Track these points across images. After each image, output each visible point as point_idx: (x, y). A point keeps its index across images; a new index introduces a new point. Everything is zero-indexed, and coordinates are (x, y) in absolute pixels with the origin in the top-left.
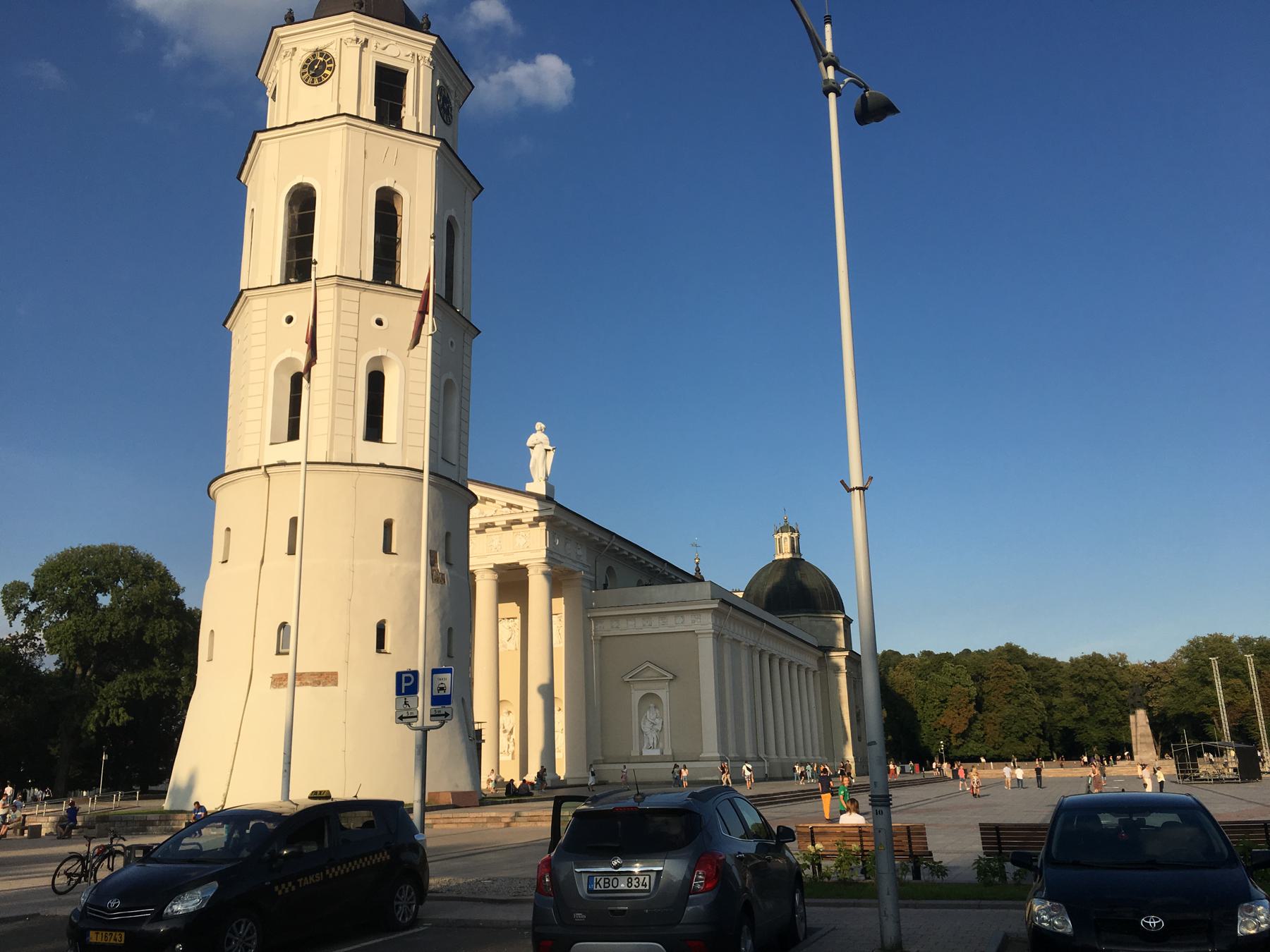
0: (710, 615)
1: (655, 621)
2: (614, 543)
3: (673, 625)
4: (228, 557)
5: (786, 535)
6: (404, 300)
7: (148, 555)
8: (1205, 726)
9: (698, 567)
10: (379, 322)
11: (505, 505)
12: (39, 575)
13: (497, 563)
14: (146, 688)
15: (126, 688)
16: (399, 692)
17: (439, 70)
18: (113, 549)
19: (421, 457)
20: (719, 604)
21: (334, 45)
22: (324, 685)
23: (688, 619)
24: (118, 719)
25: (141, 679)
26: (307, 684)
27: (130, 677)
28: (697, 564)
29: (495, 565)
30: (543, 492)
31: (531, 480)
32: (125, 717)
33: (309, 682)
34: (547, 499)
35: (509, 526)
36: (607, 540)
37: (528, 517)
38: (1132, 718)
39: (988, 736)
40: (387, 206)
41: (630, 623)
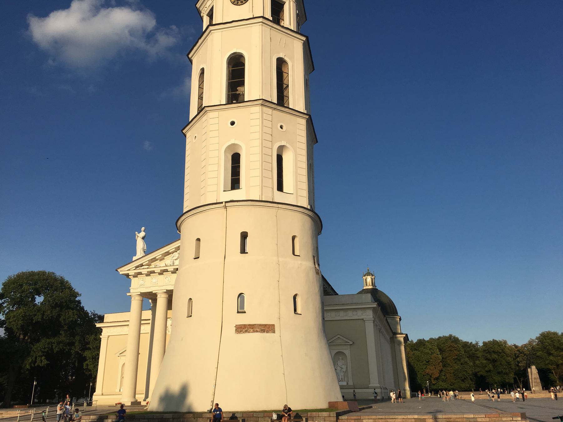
1: (342, 313)
3: (351, 315)
4: (199, 255)
7: (61, 277)
8: (549, 375)
14: (56, 346)
15: (46, 346)
18: (44, 273)
20: (377, 305)
23: (360, 312)
24: (41, 363)
25: (55, 341)
26: (257, 331)
27: (48, 341)
32: (45, 362)
33: (258, 330)
38: (529, 370)
39: (448, 379)
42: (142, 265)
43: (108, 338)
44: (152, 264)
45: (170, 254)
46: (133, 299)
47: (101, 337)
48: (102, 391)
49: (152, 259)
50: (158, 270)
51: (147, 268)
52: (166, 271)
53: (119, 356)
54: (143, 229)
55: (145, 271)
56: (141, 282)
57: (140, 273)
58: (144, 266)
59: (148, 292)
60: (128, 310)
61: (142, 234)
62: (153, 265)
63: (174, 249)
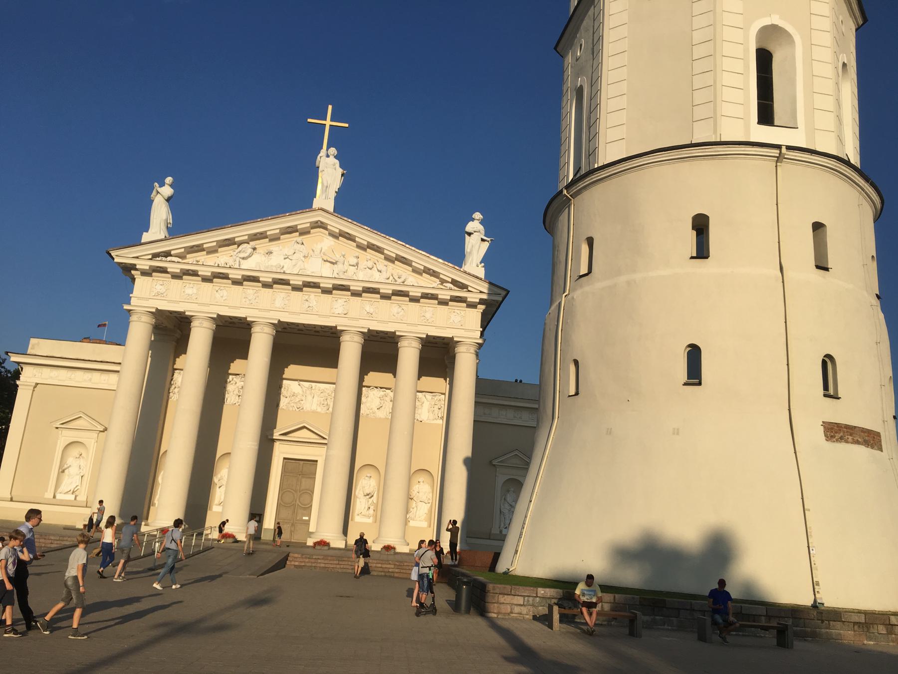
11: (450, 280)
42: (167, 254)
43: (35, 387)
44: (188, 256)
45: (234, 243)
46: (134, 318)
47: (18, 382)
48: (11, 493)
49: (194, 246)
50: (206, 272)
51: (178, 262)
52: (225, 277)
53: (57, 428)
54: (169, 180)
55: (175, 268)
56: (159, 288)
57: (163, 270)
58: (171, 255)
59: (169, 311)
60: (120, 341)
61: (167, 191)
62: (191, 258)
63: (246, 237)
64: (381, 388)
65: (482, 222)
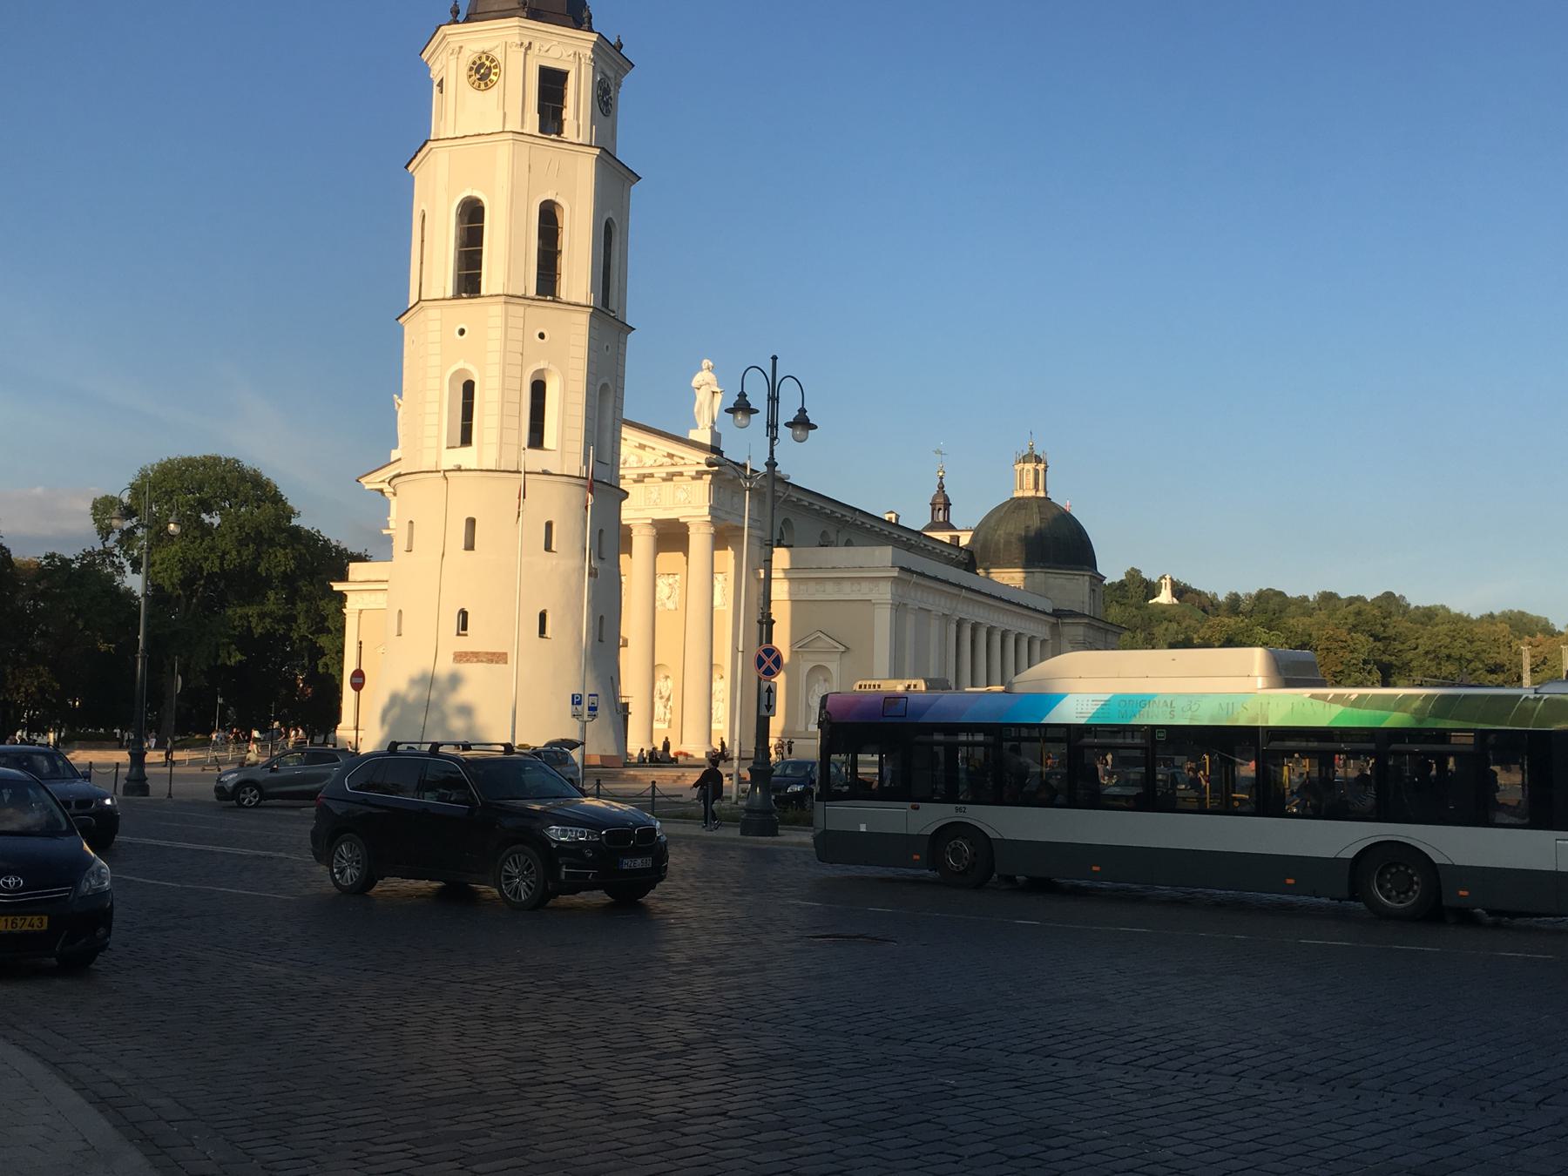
0: (890, 583)
2: (791, 494)
3: (849, 592)
4: (412, 546)
5: (1030, 467)
6: (566, 313)
7: (255, 470)
9: (941, 482)
10: (542, 336)
11: (666, 455)
12: (136, 490)
13: (656, 518)
14: (257, 625)
16: (573, 704)
17: (600, 63)
19: (574, 463)
21: (499, 48)
22: (497, 662)
23: (865, 586)
24: (229, 658)
26: (482, 661)
28: (941, 478)
29: (653, 519)
30: (706, 439)
31: (696, 427)
33: (484, 660)
34: (715, 449)
35: (669, 477)
36: (782, 490)
37: (690, 471)
40: (549, 217)
41: (802, 587)
64: (669, 574)
65: (711, 369)
